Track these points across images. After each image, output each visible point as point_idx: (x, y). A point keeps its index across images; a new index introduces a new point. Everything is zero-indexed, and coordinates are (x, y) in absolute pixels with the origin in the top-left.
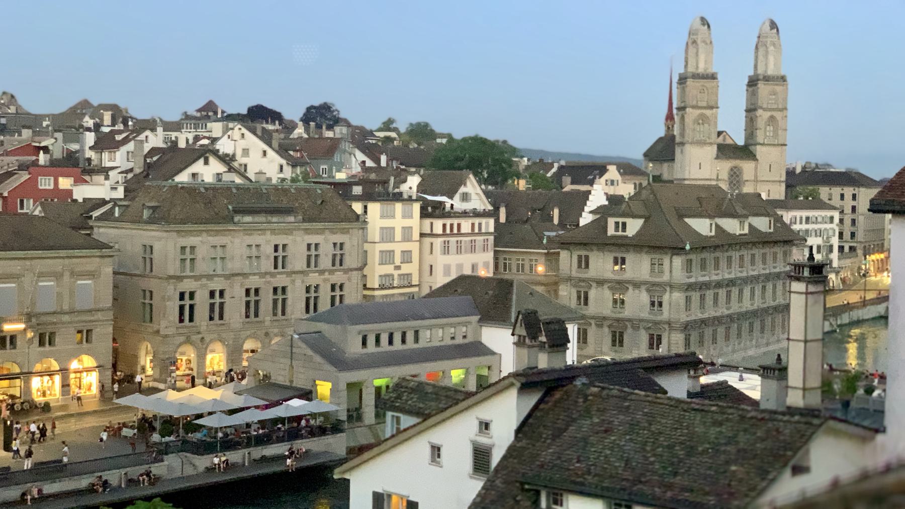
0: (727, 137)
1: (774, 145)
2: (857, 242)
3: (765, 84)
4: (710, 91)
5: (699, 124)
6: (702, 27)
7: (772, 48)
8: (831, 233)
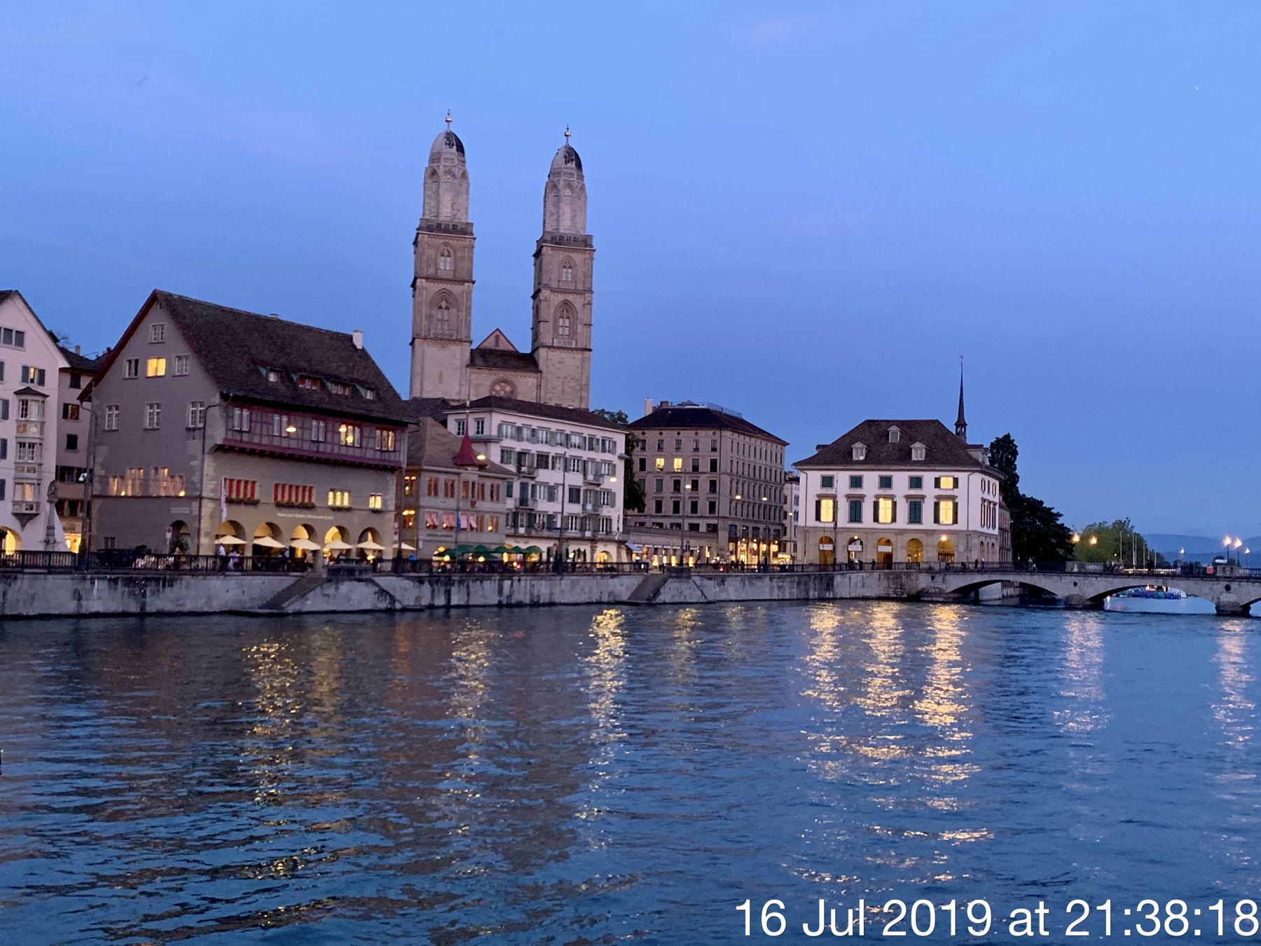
0: (501, 337)
1: (572, 349)
2: (718, 517)
3: (553, 248)
4: (459, 254)
5: (440, 307)
6: (447, 149)
7: (567, 192)
8: (605, 469)
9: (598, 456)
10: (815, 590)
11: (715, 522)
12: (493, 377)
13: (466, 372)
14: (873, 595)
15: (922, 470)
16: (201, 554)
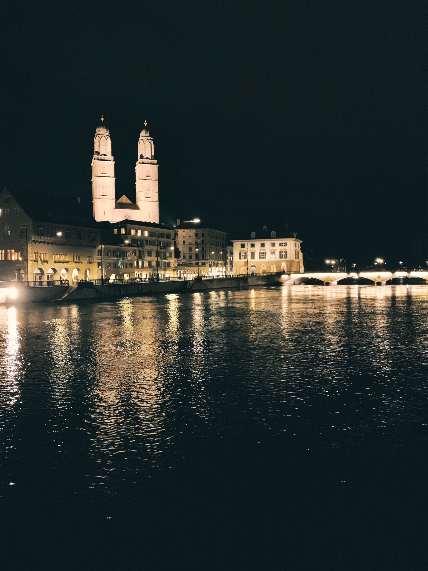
9: (165, 240)
10: (242, 283)
11: (204, 261)
14: (260, 284)
15: (276, 241)
16: (29, 280)
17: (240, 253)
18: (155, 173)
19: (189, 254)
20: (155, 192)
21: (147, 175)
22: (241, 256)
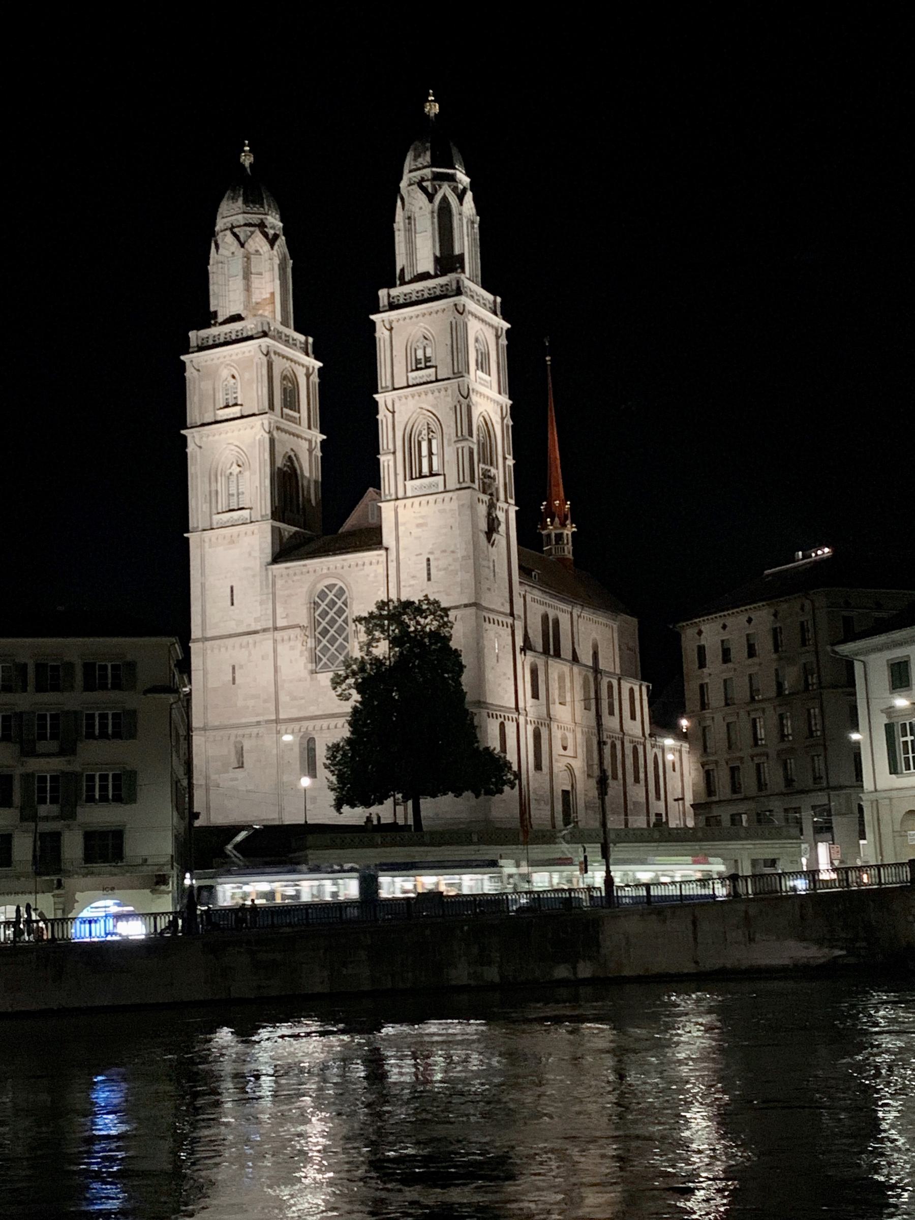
12: (312, 578)
13: (267, 575)
17: (889, 728)
18: (449, 343)
19: (752, 757)
20: (454, 438)
21: (418, 361)
22: (900, 749)
